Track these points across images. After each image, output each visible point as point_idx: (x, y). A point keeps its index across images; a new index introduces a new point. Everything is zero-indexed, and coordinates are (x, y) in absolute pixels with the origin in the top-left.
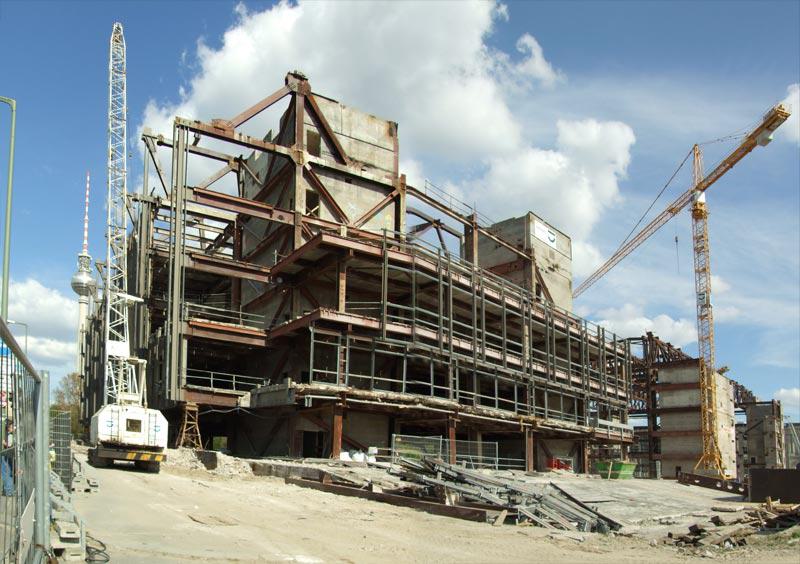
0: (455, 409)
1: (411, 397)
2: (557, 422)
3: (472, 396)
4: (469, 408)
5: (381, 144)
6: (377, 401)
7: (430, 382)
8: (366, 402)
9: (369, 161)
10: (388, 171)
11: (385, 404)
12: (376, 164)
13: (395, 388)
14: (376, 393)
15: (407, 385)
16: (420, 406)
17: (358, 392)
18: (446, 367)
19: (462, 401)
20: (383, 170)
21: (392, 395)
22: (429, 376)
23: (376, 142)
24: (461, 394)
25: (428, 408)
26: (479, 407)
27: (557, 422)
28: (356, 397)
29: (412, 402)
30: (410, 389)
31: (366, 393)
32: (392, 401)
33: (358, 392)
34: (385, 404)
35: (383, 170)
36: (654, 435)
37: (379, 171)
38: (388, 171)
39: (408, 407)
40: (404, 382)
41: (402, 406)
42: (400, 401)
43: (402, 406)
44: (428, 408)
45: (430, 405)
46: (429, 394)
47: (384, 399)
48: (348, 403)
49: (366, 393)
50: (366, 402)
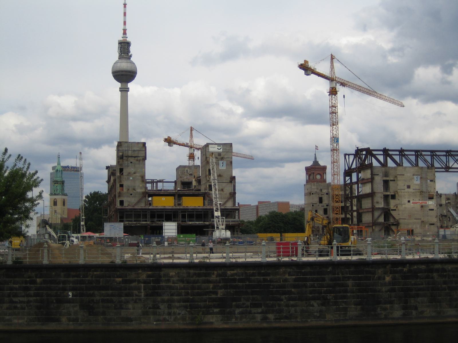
0: (149, 224)
2: (190, 223)
3: (155, 220)
4: (154, 223)
12: (140, 155)
13: (131, 221)
16: (138, 225)
19: (151, 222)
23: (138, 149)
24: (151, 220)
26: (157, 222)
27: (190, 223)
30: (135, 221)
32: (131, 224)
36: (360, 211)
37: (141, 157)
39: (134, 225)
41: (133, 225)
47: (128, 224)
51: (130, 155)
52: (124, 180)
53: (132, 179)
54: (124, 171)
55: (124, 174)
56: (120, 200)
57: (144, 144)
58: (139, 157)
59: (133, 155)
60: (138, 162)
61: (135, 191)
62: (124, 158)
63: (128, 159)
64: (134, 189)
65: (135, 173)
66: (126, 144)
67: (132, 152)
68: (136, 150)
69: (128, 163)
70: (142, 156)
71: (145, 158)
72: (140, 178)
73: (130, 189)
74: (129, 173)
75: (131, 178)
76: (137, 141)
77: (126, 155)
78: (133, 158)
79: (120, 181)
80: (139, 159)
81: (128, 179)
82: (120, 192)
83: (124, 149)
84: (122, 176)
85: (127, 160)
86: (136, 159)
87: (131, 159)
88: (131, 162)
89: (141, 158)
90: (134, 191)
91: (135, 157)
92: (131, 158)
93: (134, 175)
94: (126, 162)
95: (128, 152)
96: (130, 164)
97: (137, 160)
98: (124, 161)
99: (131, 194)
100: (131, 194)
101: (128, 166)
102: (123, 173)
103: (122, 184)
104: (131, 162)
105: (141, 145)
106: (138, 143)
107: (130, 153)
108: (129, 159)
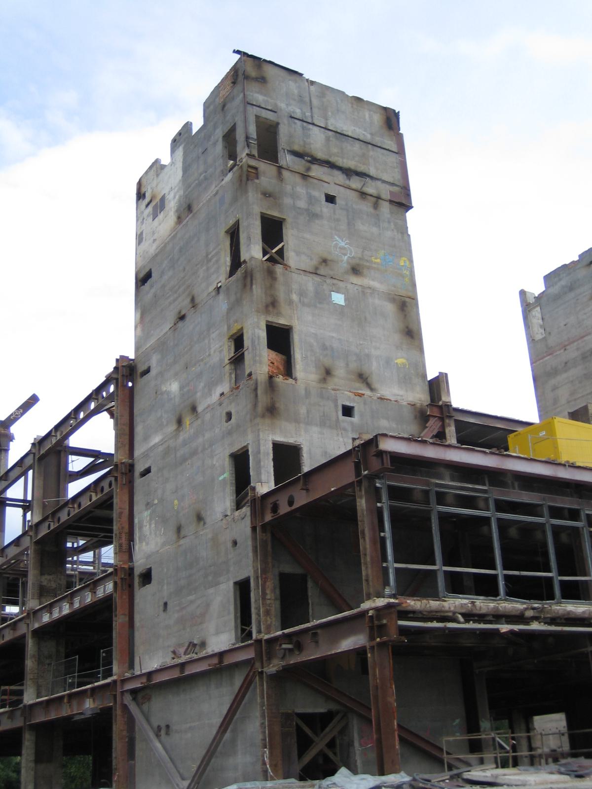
1: (517, 606)
5: (377, 140)
6: (454, 620)
7: (549, 570)
8: (435, 624)
9: (362, 168)
10: (393, 184)
11: (471, 625)
12: (372, 172)
13: (486, 587)
14: (455, 603)
15: (507, 578)
16: (535, 626)
17: (413, 603)
18: (576, 530)
20: (384, 182)
21: (483, 604)
22: (546, 554)
23: (359, 132)
25: (553, 628)
28: (405, 614)
29: (519, 618)
30: (517, 589)
31: (434, 604)
32: (481, 618)
33: (413, 603)
34: (471, 625)
35: (384, 182)
37: (379, 183)
38: (393, 184)
40: (500, 572)
41: (504, 628)
42: (498, 617)
43: (504, 628)
44: (553, 628)
45: (553, 621)
46: (551, 597)
47: (469, 616)
48: (403, 631)
49: (434, 604)
50: (435, 624)
51: (320, 155)
52: (295, 297)
53: (342, 302)
54: (291, 238)
55: (291, 257)
56: (280, 439)
57: (391, 119)
58: (372, 178)
59: (340, 162)
60: (365, 207)
61: (372, 389)
62: (286, 159)
63: (308, 169)
64: (363, 378)
65: (356, 270)
66: (292, 85)
67: (328, 139)
68: (350, 134)
69: (307, 193)
70: (385, 177)
71: (403, 203)
72: (390, 308)
73: (340, 371)
74: (325, 261)
75: (338, 299)
76: (351, 91)
77: (296, 148)
78: (340, 177)
79: (272, 304)
80: (370, 189)
81: (322, 298)
82: (271, 377)
83: (282, 105)
84: (279, 269)
85: (305, 177)
86: (356, 183)
87: (334, 182)
88: (330, 199)
89: (385, 191)
90: (367, 392)
91: (349, 172)
92: (326, 169)
93: (355, 279)
94: (301, 190)
95: (303, 128)
96: (326, 208)
97: (363, 195)
98: (286, 174)
99: (348, 411)
100: (348, 411)
101: (314, 216)
102: (281, 253)
103: (282, 321)
104: (330, 199)
105: (378, 119)
106: (358, 100)
107: (317, 142)
108: (317, 171)
